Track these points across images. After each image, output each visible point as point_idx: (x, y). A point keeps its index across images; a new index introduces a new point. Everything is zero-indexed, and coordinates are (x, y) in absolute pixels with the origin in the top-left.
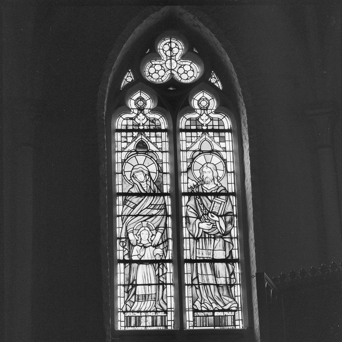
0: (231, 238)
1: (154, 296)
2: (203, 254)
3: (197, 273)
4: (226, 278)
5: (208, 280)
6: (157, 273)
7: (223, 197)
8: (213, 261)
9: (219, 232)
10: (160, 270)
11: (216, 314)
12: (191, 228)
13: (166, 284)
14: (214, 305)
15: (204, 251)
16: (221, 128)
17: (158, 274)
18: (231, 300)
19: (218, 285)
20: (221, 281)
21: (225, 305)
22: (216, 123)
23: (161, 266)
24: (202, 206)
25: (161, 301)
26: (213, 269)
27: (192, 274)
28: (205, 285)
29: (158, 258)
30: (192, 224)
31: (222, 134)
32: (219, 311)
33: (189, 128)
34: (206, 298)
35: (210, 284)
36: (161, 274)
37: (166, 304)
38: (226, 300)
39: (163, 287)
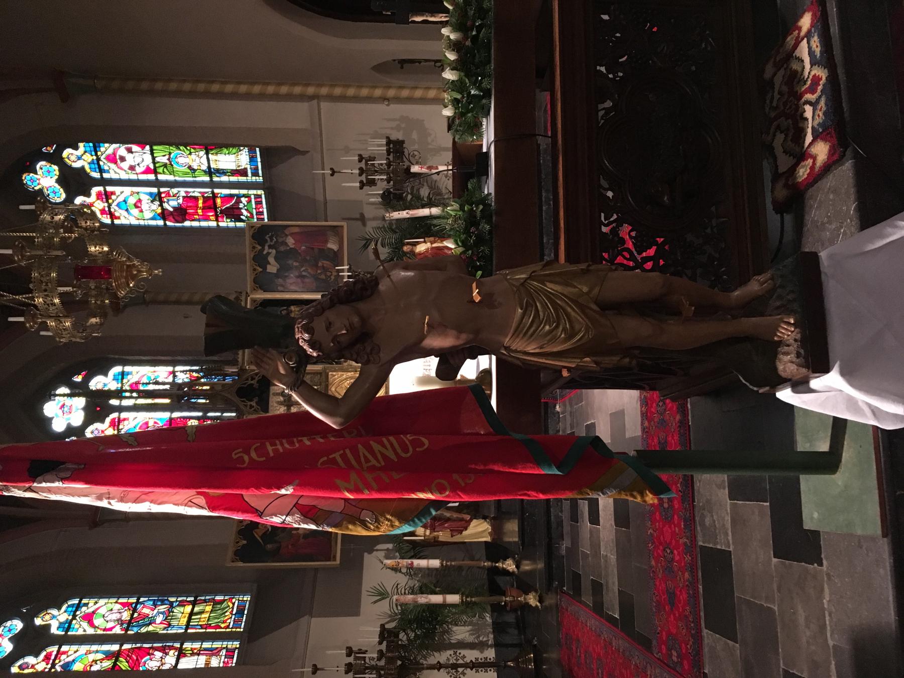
0: (177, 601)
1: (208, 657)
2: (184, 621)
3: (197, 625)
4: (207, 605)
5: (205, 618)
6: (189, 655)
7: (138, 606)
8: (192, 614)
9: (168, 610)
10: (187, 652)
11: (234, 612)
12: (158, 630)
13: (201, 647)
14: (227, 614)
15: (182, 620)
16: (75, 606)
17: (190, 654)
18: (226, 602)
19: (212, 611)
20: (209, 608)
21: (229, 606)
22: (70, 609)
23: (184, 652)
24: (140, 622)
25: (214, 652)
26: (197, 614)
27: (196, 629)
28: (208, 620)
29: (176, 653)
30: (154, 629)
31: (81, 605)
32: (232, 611)
33: (65, 629)
34: (219, 620)
35: (209, 616)
36: (191, 652)
37: (217, 648)
38: (224, 605)
39: (202, 650)
